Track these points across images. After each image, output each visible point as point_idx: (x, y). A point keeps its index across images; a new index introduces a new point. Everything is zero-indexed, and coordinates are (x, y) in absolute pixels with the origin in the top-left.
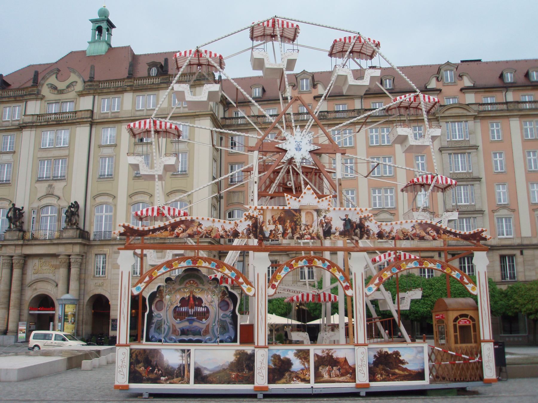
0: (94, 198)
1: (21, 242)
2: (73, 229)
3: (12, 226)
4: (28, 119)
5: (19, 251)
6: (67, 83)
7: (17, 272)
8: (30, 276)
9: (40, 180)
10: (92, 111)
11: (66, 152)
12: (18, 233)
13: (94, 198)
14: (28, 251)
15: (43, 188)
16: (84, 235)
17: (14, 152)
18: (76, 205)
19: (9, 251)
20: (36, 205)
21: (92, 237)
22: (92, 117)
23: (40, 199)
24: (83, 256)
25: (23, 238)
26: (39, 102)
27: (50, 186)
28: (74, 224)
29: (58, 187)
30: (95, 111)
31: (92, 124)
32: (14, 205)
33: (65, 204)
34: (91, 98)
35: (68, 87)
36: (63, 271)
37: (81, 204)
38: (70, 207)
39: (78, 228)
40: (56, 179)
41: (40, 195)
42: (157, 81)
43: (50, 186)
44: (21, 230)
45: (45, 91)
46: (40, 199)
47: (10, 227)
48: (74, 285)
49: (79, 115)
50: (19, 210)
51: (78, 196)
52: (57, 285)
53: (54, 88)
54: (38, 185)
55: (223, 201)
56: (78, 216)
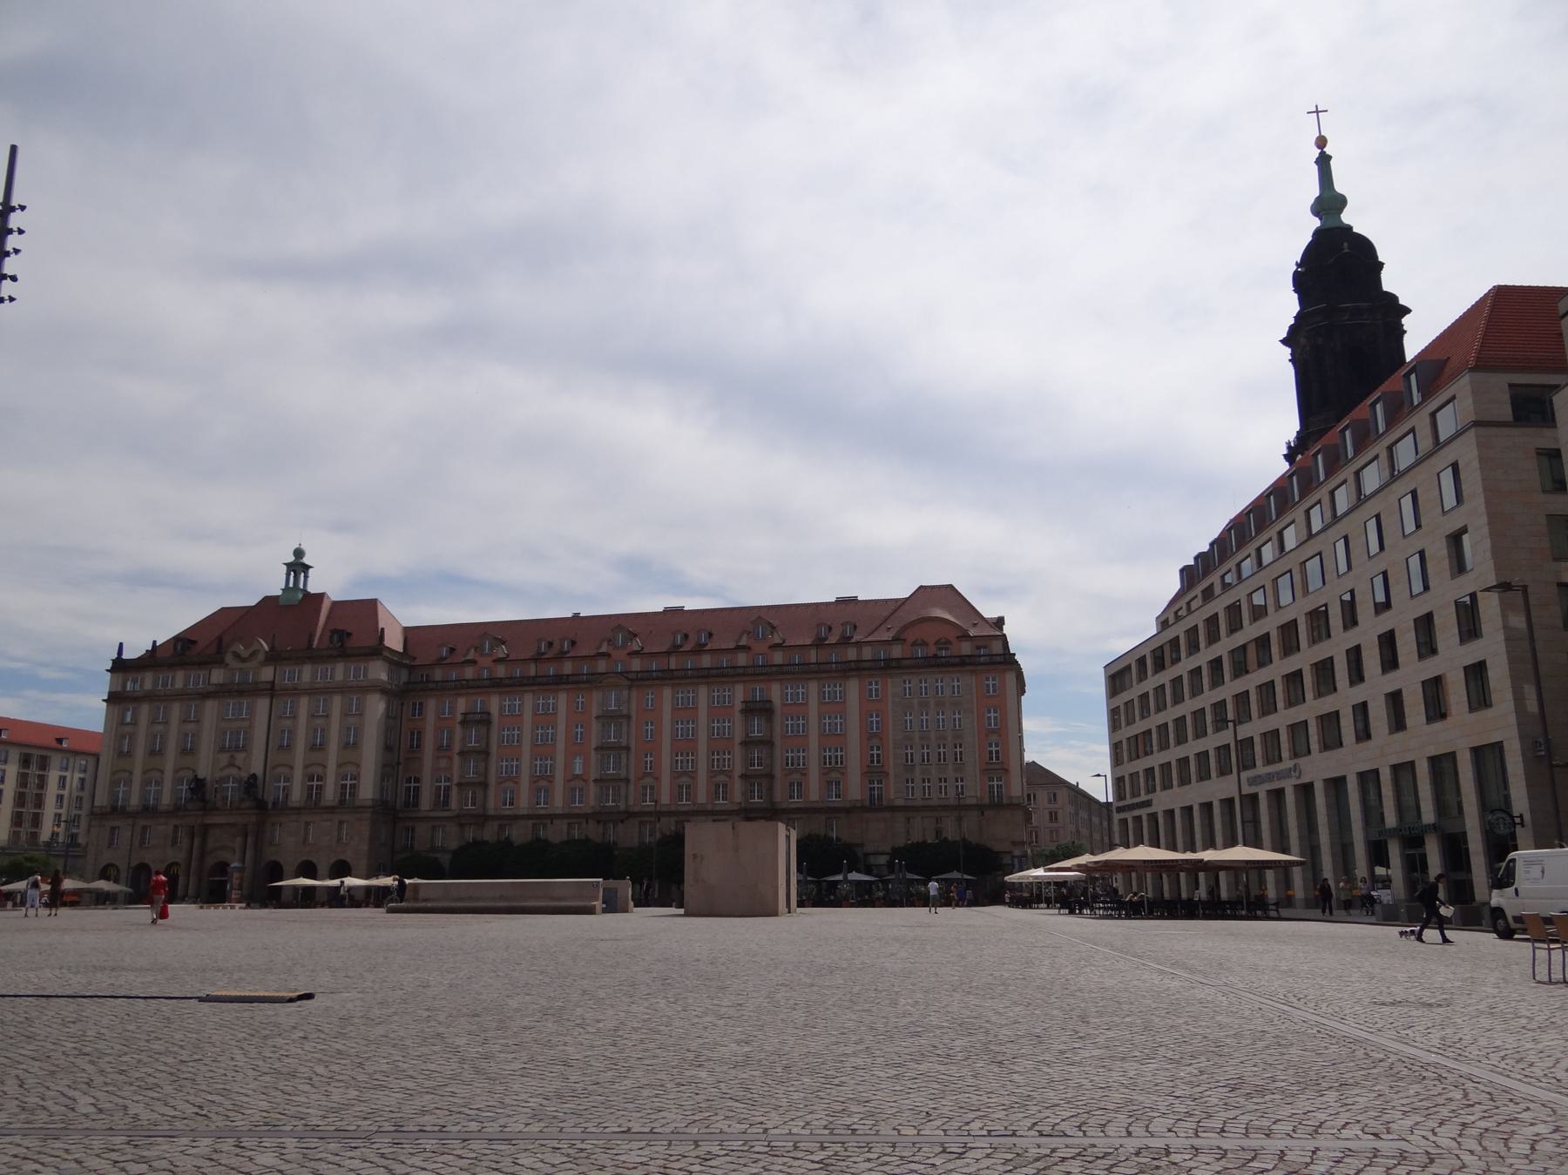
0: (273, 768)
1: (201, 813)
3: (195, 797)
4: (211, 689)
6: (251, 650)
9: (222, 750)
10: (274, 682)
13: (273, 768)
16: (261, 805)
17: (198, 721)
18: (254, 776)
20: (218, 775)
21: (270, 806)
26: (222, 671)
27: (232, 757)
29: (240, 757)
30: (276, 682)
33: (245, 775)
35: (251, 655)
38: (249, 778)
40: (237, 749)
43: (232, 757)
44: (203, 800)
45: (229, 658)
46: (221, 770)
47: (192, 798)
51: (257, 767)
53: (237, 656)
55: (400, 767)
56: (256, 787)
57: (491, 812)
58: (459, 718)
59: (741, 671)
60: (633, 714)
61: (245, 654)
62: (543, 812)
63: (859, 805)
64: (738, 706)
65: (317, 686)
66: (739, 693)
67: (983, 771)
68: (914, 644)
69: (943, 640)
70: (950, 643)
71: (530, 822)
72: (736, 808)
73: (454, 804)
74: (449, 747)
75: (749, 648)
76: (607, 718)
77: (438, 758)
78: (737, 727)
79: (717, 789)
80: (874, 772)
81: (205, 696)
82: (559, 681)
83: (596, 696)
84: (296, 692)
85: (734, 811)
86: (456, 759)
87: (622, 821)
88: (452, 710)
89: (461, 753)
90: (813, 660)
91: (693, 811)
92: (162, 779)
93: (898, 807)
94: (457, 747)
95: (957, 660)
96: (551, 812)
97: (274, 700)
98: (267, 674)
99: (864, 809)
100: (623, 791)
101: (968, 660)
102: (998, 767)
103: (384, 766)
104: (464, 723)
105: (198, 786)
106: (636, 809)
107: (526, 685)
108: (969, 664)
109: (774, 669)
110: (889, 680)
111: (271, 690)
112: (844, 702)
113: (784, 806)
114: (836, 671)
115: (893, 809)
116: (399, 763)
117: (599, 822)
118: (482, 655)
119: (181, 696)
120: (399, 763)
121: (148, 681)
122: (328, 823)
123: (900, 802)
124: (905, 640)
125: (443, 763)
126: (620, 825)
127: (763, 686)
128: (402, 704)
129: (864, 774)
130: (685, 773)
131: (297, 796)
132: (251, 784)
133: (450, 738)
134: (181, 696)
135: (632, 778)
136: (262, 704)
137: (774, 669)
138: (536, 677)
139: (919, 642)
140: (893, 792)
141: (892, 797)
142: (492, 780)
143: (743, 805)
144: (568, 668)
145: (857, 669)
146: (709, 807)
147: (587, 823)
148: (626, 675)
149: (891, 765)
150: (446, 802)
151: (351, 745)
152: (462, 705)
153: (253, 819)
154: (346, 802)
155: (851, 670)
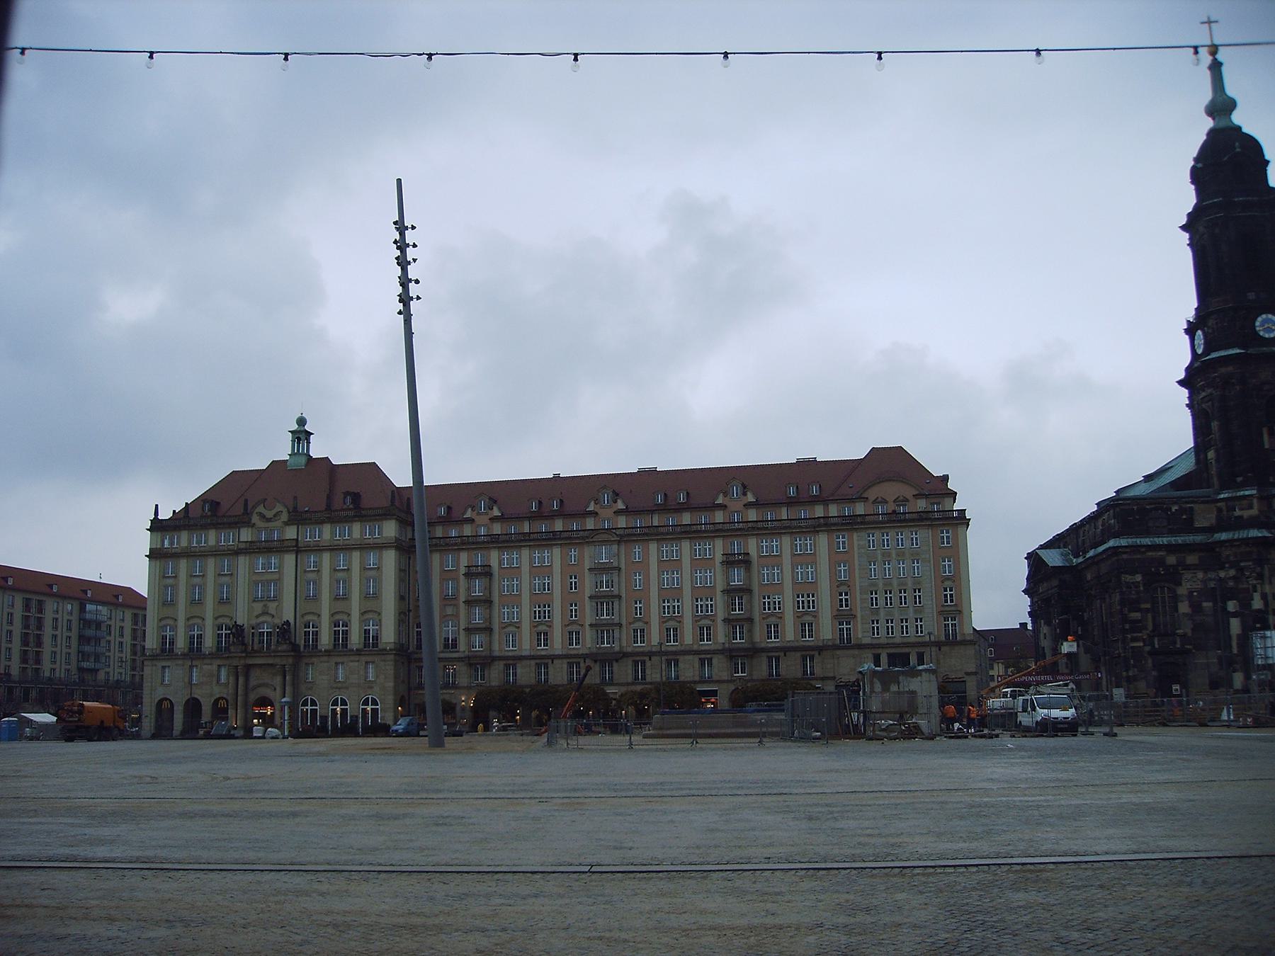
0: (303, 616)
1: (244, 655)
2: (286, 643)
5: (242, 662)
7: (241, 680)
8: (253, 682)
10: (297, 540)
11: (276, 577)
12: (240, 647)
13: (303, 616)
14: (250, 662)
15: (258, 607)
16: (295, 647)
18: (288, 623)
19: (235, 662)
20: (254, 622)
22: (297, 546)
23: (257, 617)
24: (295, 667)
25: (245, 651)
27: (265, 606)
28: (287, 639)
29: (272, 606)
30: (299, 539)
31: (297, 552)
32: (236, 622)
34: (296, 527)
36: (278, 679)
37: (292, 621)
38: (283, 625)
39: (291, 643)
40: (269, 599)
41: (256, 613)
42: (351, 513)
46: (257, 617)
48: (288, 689)
49: (286, 544)
50: (240, 626)
51: (288, 615)
52: (275, 689)
54: (255, 605)
55: (411, 614)
56: (290, 632)
57: (497, 654)
58: (463, 570)
59: (720, 527)
60: (623, 566)
61: (269, 514)
62: (543, 653)
63: (830, 643)
64: (719, 558)
65: (336, 543)
66: (718, 548)
67: (940, 613)
68: (875, 502)
69: (902, 498)
70: (907, 500)
71: (533, 662)
72: (720, 648)
73: (462, 646)
74: (455, 597)
75: (726, 506)
76: (598, 569)
77: (445, 605)
78: (717, 578)
79: (704, 631)
80: (843, 616)
81: (237, 553)
82: (552, 539)
83: (588, 551)
84: (318, 549)
85: (718, 650)
86: (462, 606)
87: (617, 661)
88: (457, 563)
89: (468, 602)
90: (785, 517)
91: (682, 651)
92: (204, 625)
93: (864, 645)
94: (462, 598)
95: (915, 516)
96: (552, 653)
97: (299, 557)
98: (291, 533)
99: (835, 647)
100: (617, 635)
101: (924, 516)
102: (953, 608)
103: (400, 614)
104: (468, 575)
105: (238, 631)
106: (629, 650)
107: (523, 540)
108: (926, 519)
109: (750, 525)
110: (855, 535)
111: (297, 548)
112: (815, 554)
113: (763, 645)
114: (806, 527)
115: (861, 647)
116: (409, 611)
117: (596, 661)
118: (479, 514)
119: (217, 553)
120: (409, 611)
121: (183, 540)
122: (356, 664)
123: (867, 641)
124: (867, 498)
125: (449, 611)
126: (615, 665)
127: (741, 540)
128: (410, 558)
129: (835, 617)
130: (671, 618)
131: (325, 640)
132: (285, 631)
133: (456, 589)
134: (217, 553)
135: (624, 622)
136: (290, 559)
137: (750, 525)
138: (530, 533)
139: (880, 499)
140: (861, 633)
141: (860, 636)
142: (496, 627)
143: (727, 645)
144: (559, 525)
145: (826, 525)
146: (695, 647)
147: (585, 662)
148: (614, 531)
149: (859, 610)
150: (455, 645)
151: (371, 597)
152: (464, 558)
153: (290, 660)
154: (371, 644)
155: (819, 526)
